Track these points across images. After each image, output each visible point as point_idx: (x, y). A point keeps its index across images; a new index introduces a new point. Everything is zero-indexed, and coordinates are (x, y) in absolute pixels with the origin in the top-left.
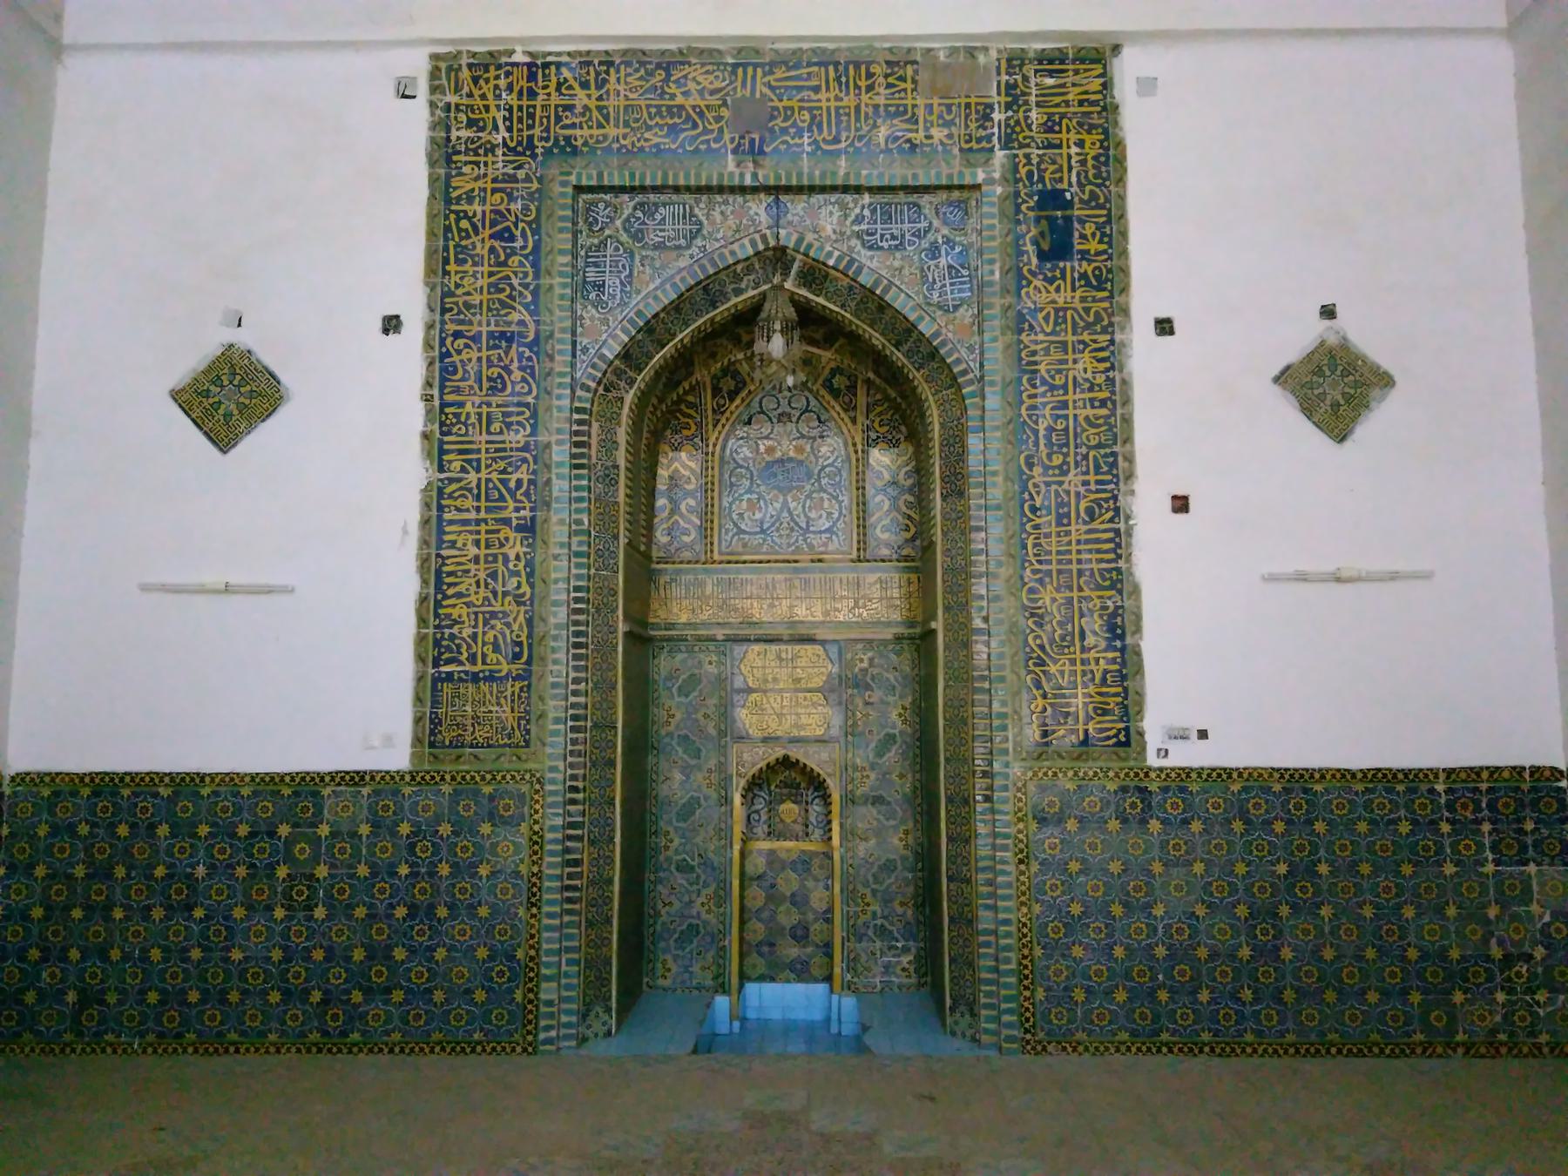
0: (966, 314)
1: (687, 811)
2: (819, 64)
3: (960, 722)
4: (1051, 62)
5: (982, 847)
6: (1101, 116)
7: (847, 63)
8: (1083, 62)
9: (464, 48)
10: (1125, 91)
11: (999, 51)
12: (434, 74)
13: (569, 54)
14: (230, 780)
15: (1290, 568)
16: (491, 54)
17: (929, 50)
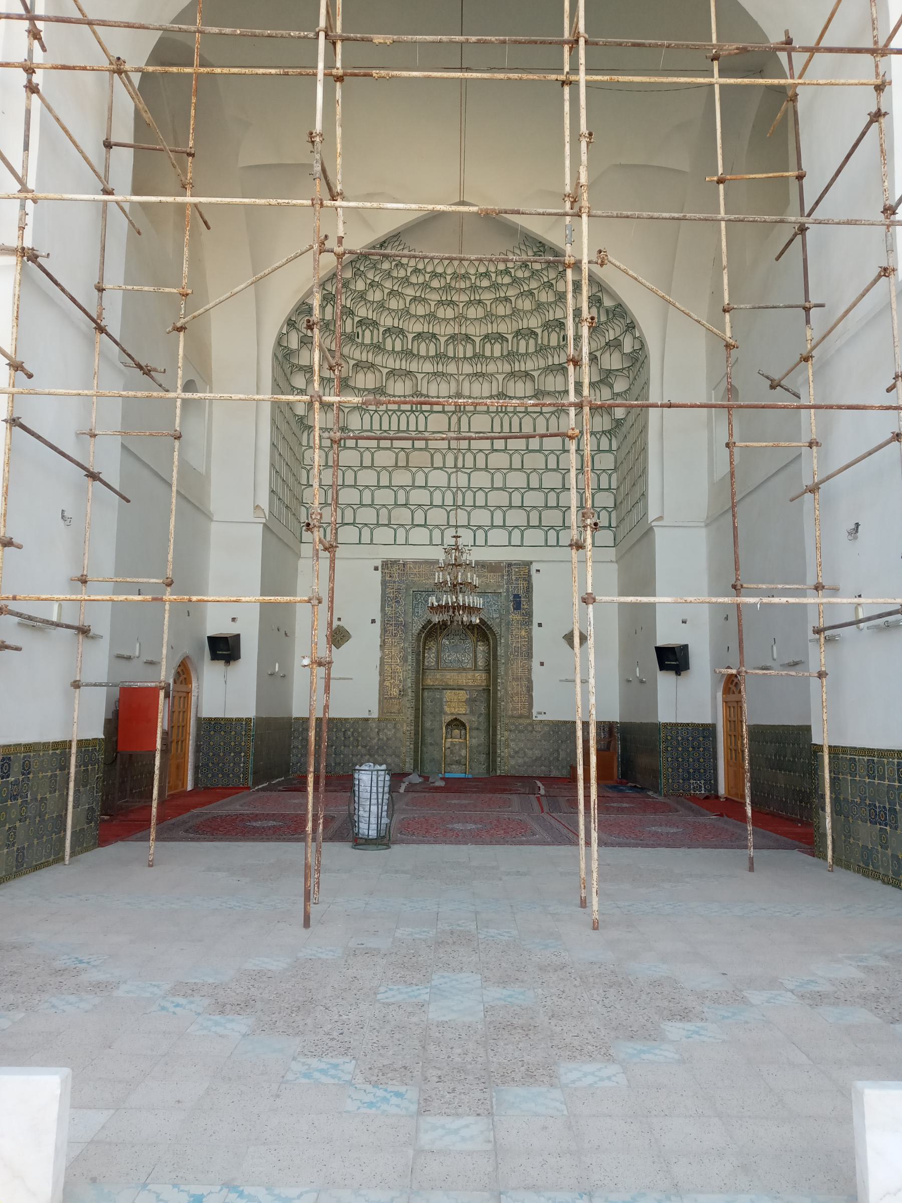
0: (498, 620)
1: (432, 730)
3: (495, 710)
5: (499, 737)
6: (528, 579)
10: (533, 572)
12: (382, 565)
14: (340, 719)
15: (563, 679)
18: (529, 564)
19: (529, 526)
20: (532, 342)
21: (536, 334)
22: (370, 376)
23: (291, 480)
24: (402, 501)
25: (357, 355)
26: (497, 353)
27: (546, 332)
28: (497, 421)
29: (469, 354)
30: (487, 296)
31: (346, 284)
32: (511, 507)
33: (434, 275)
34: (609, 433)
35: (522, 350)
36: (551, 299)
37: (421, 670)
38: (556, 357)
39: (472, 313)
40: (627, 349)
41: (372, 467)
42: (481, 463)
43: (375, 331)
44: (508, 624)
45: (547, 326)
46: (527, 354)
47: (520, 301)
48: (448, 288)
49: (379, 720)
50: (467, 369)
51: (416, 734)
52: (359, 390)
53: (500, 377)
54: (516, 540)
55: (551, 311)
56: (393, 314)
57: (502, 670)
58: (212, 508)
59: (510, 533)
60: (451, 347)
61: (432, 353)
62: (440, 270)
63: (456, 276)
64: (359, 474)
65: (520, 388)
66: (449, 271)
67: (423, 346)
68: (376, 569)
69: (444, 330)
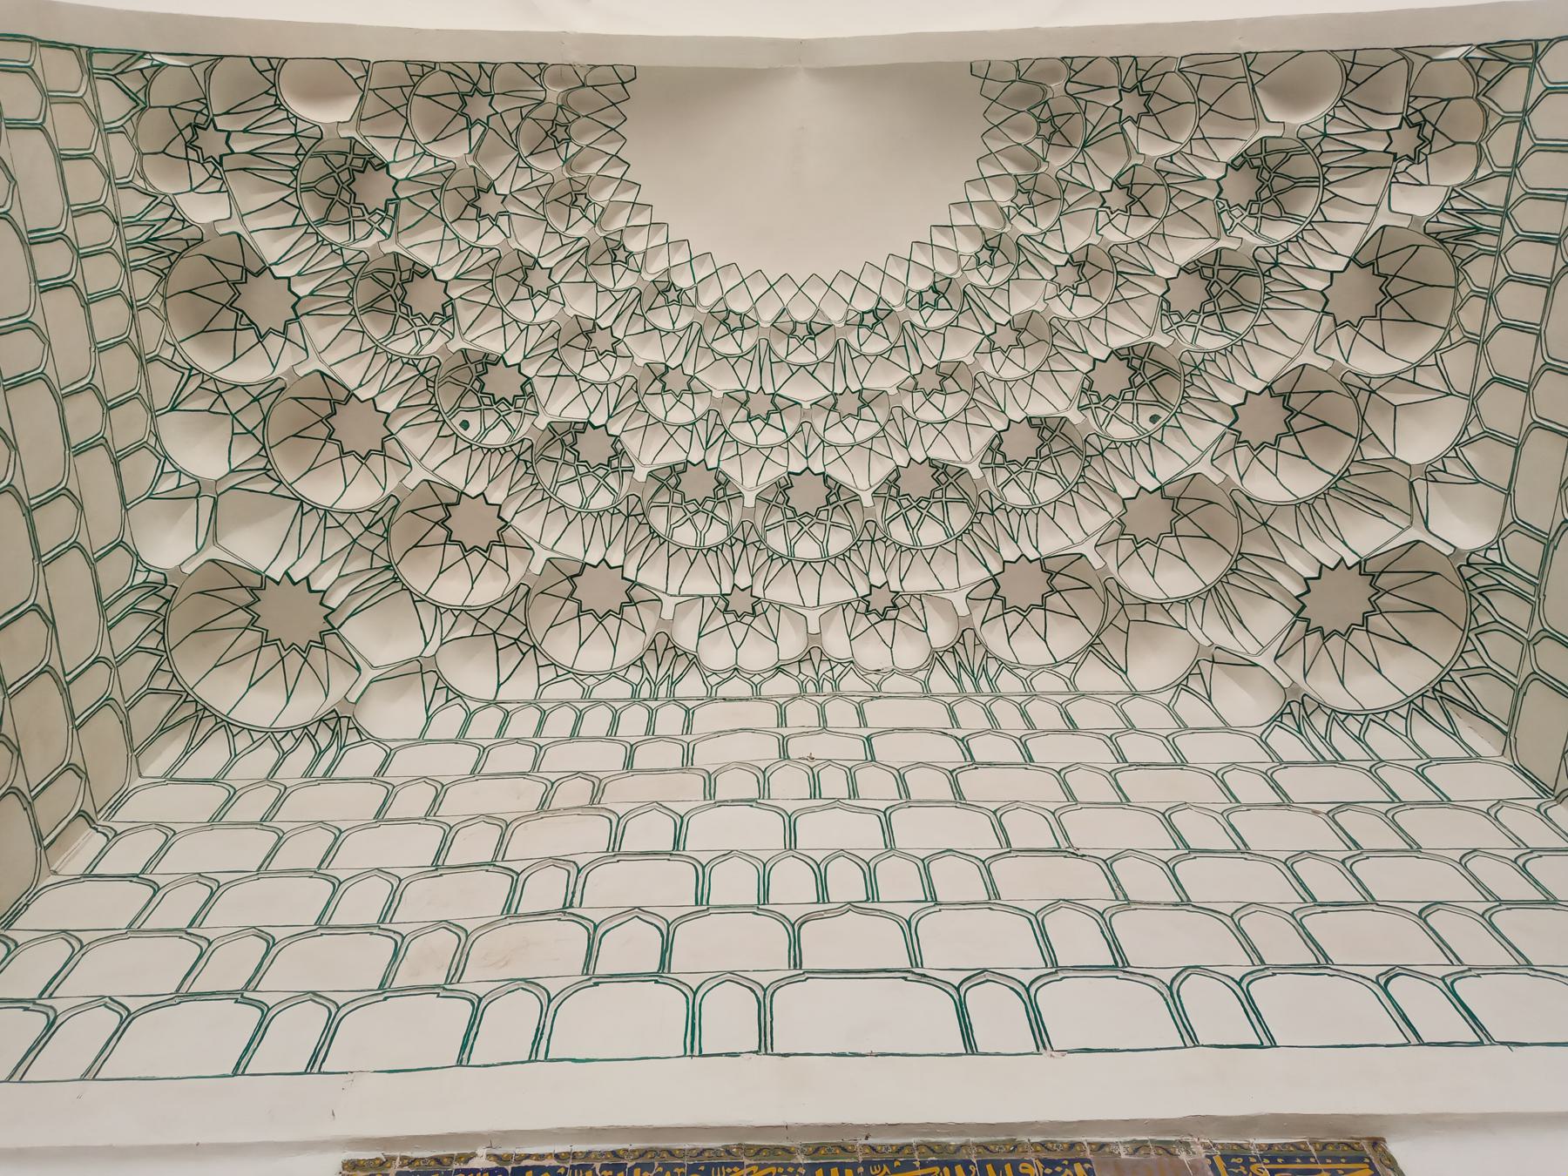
2: (941, 1164)
4: (1288, 1160)
7: (982, 1165)
8: (1336, 1160)
9: (397, 1154)
11: (1207, 1147)
13: (557, 1156)
16: (438, 1160)
17: (1102, 1146)
27: (1088, 413)
39: (838, 435)
50: (836, 591)
53: (959, 600)
56: (592, 397)
62: (740, 305)
66: (767, 317)
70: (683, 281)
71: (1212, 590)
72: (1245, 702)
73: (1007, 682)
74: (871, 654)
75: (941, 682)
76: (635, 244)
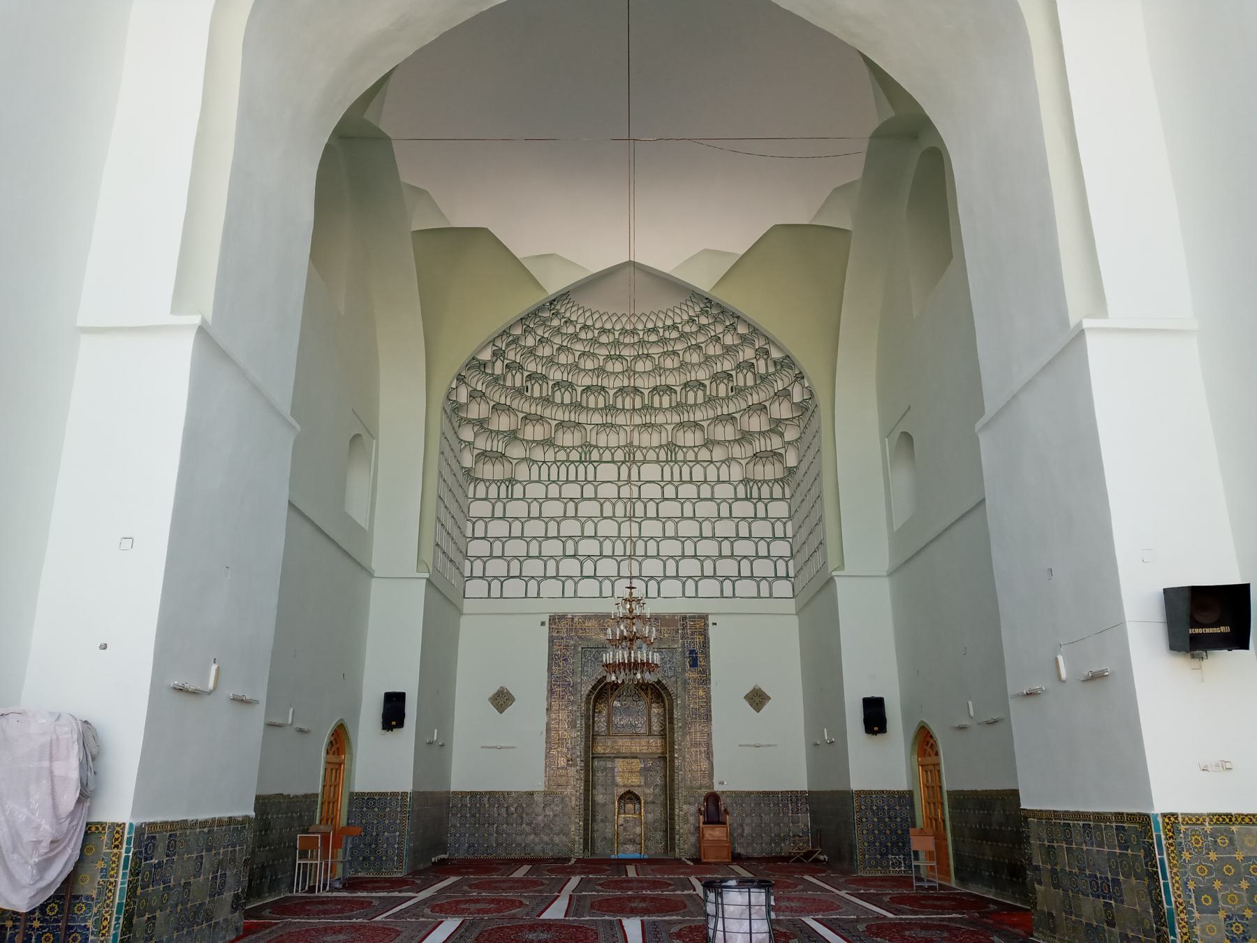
3: (672, 780)
6: (704, 634)
18: (704, 617)
19: (703, 577)
20: (700, 393)
21: (705, 386)
22: (539, 428)
23: (455, 533)
24: (570, 551)
25: (526, 408)
26: (666, 404)
28: (667, 469)
29: (638, 405)
30: (654, 350)
31: (516, 341)
32: (683, 556)
33: (603, 331)
34: (781, 481)
35: (691, 401)
36: (719, 351)
37: (591, 737)
38: (725, 407)
39: (640, 366)
40: (797, 398)
41: (540, 518)
42: (651, 512)
43: (545, 385)
44: (685, 682)
45: (715, 377)
46: (696, 405)
47: (687, 354)
48: (616, 343)
49: (545, 794)
51: (586, 809)
52: (527, 441)
53: (669, 428)
54: (690, 591)
55: (719, 364)
57: (678, 736)
58: (373, 566)
59: (684, 584)
60: (619, 399)
61: (601, 405)
62: (608, 326)
63: (624, 332)
64: (526, 524)
65: (689, 438)
66: (618, 327)
67: (592, 398)
68: (543, 624)
69: (612, 384)
70: (589, 323)
71: (735, 441)
72: (737, 473)
73: (680, 456)
74: (646, 439)
75: (663, 456)
76: (574, 318)
